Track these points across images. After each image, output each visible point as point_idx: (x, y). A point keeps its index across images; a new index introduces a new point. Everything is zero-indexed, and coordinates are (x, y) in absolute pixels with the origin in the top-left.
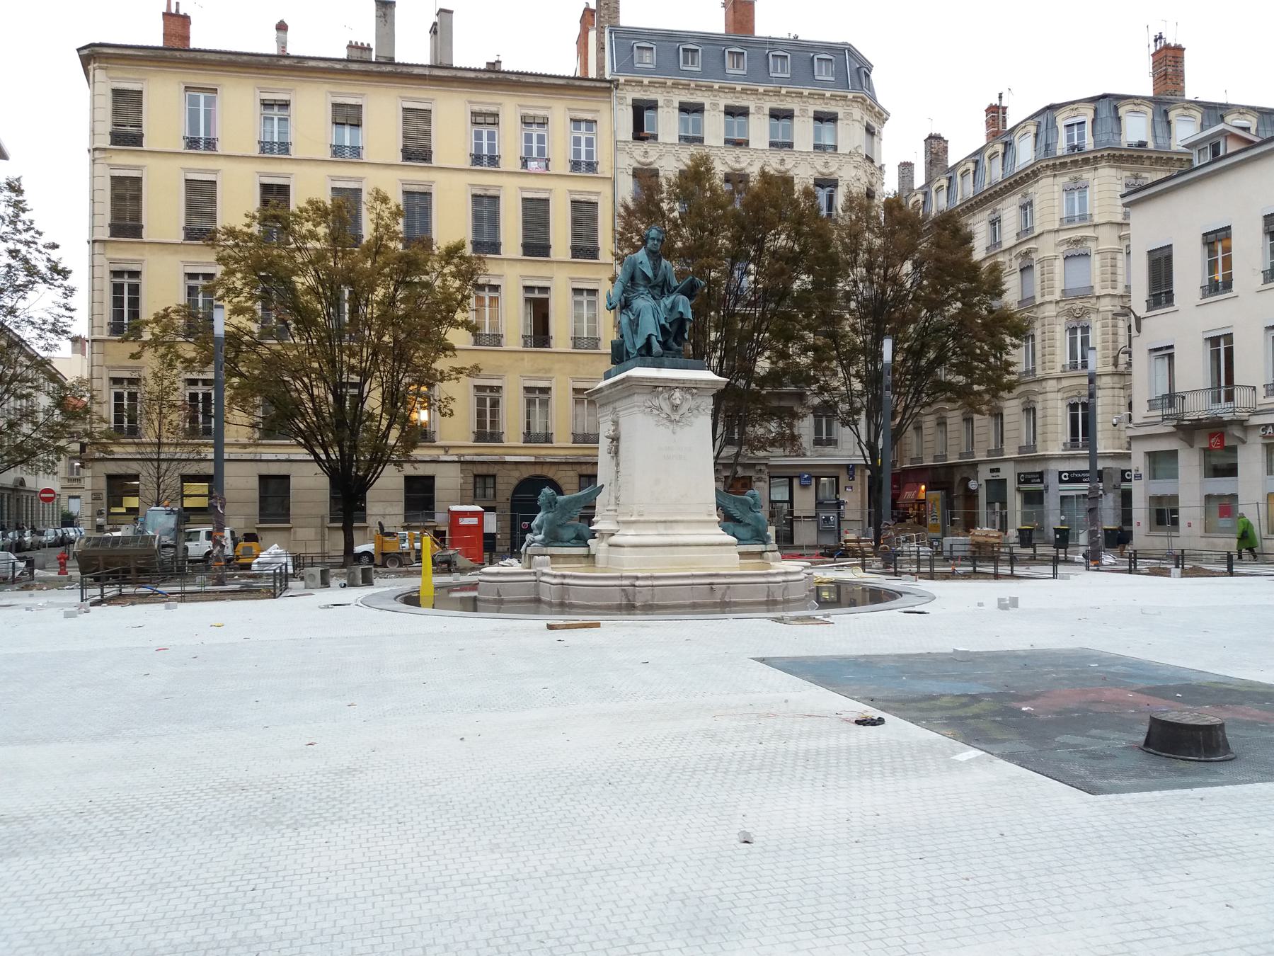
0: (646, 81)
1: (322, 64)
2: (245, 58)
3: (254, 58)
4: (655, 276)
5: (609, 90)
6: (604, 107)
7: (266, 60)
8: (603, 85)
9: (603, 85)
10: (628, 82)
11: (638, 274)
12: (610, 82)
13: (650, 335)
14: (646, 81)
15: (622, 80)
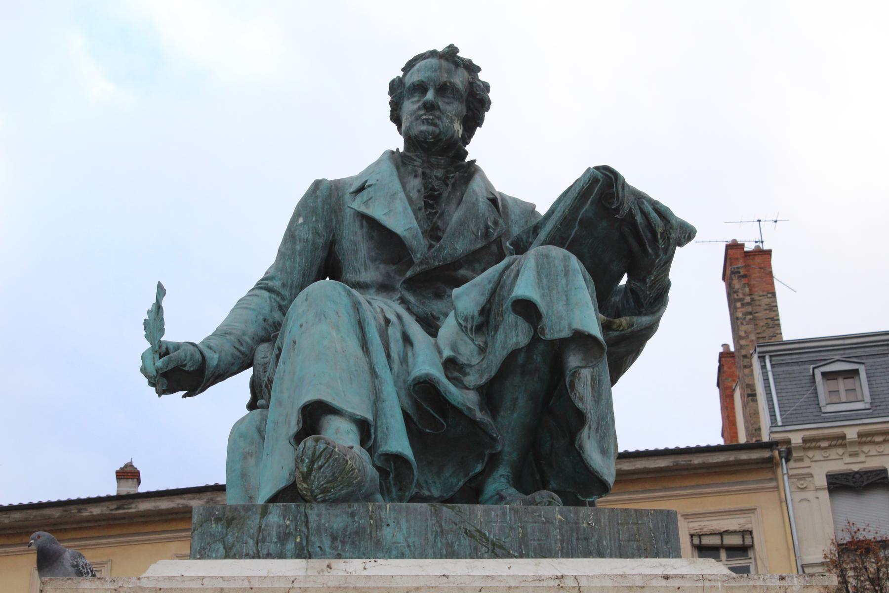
0: (851, 434)
1: (165, 504)
2: (17, 515)
3: (34, 513)
4: (433, 233)
5: (769, 465)
6: (764, 501)
7: (56, 513)
8: (755, 455)
9: (755, 455)
10: (810, 443)
11: (354, 239)
12: (771, 445)
13: (314, 416)
14: (851, 434)
15: (796, 439)
